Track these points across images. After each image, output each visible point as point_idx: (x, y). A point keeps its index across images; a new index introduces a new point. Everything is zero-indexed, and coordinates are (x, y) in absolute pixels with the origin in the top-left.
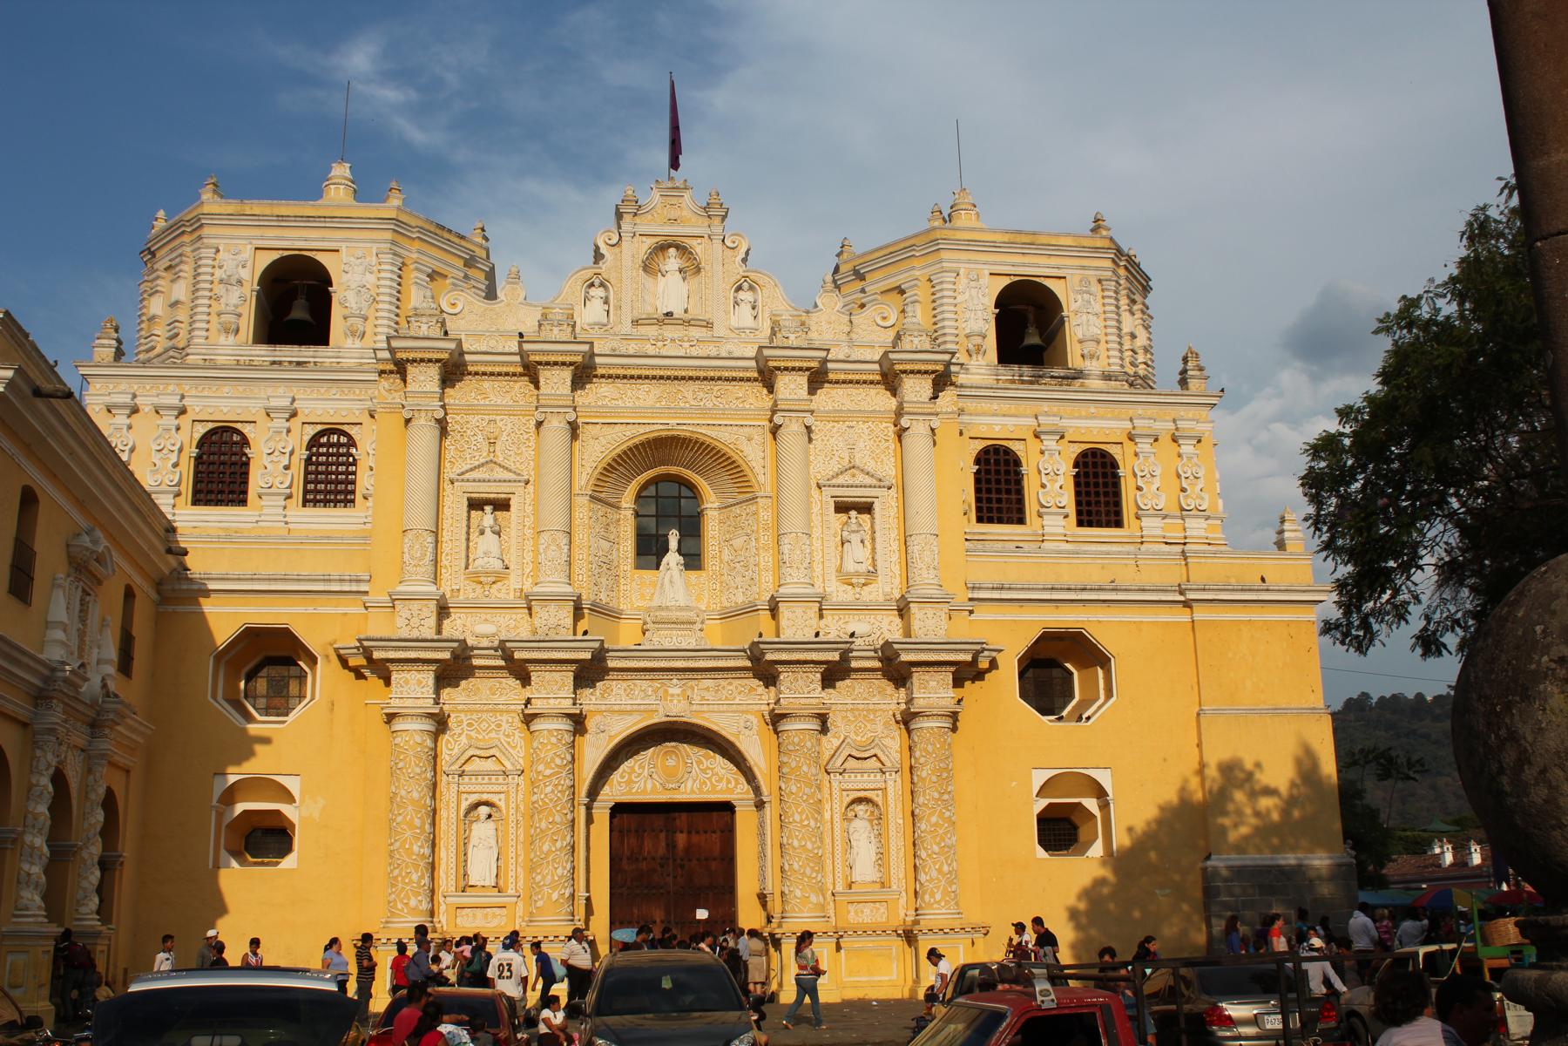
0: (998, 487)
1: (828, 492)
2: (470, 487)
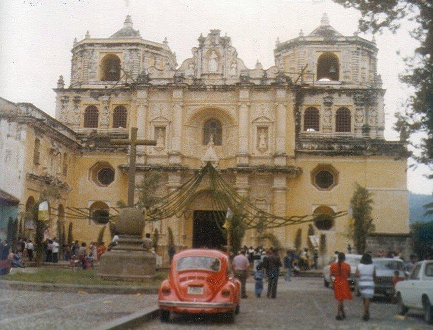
1: (255, 124)
2: (155, 124)
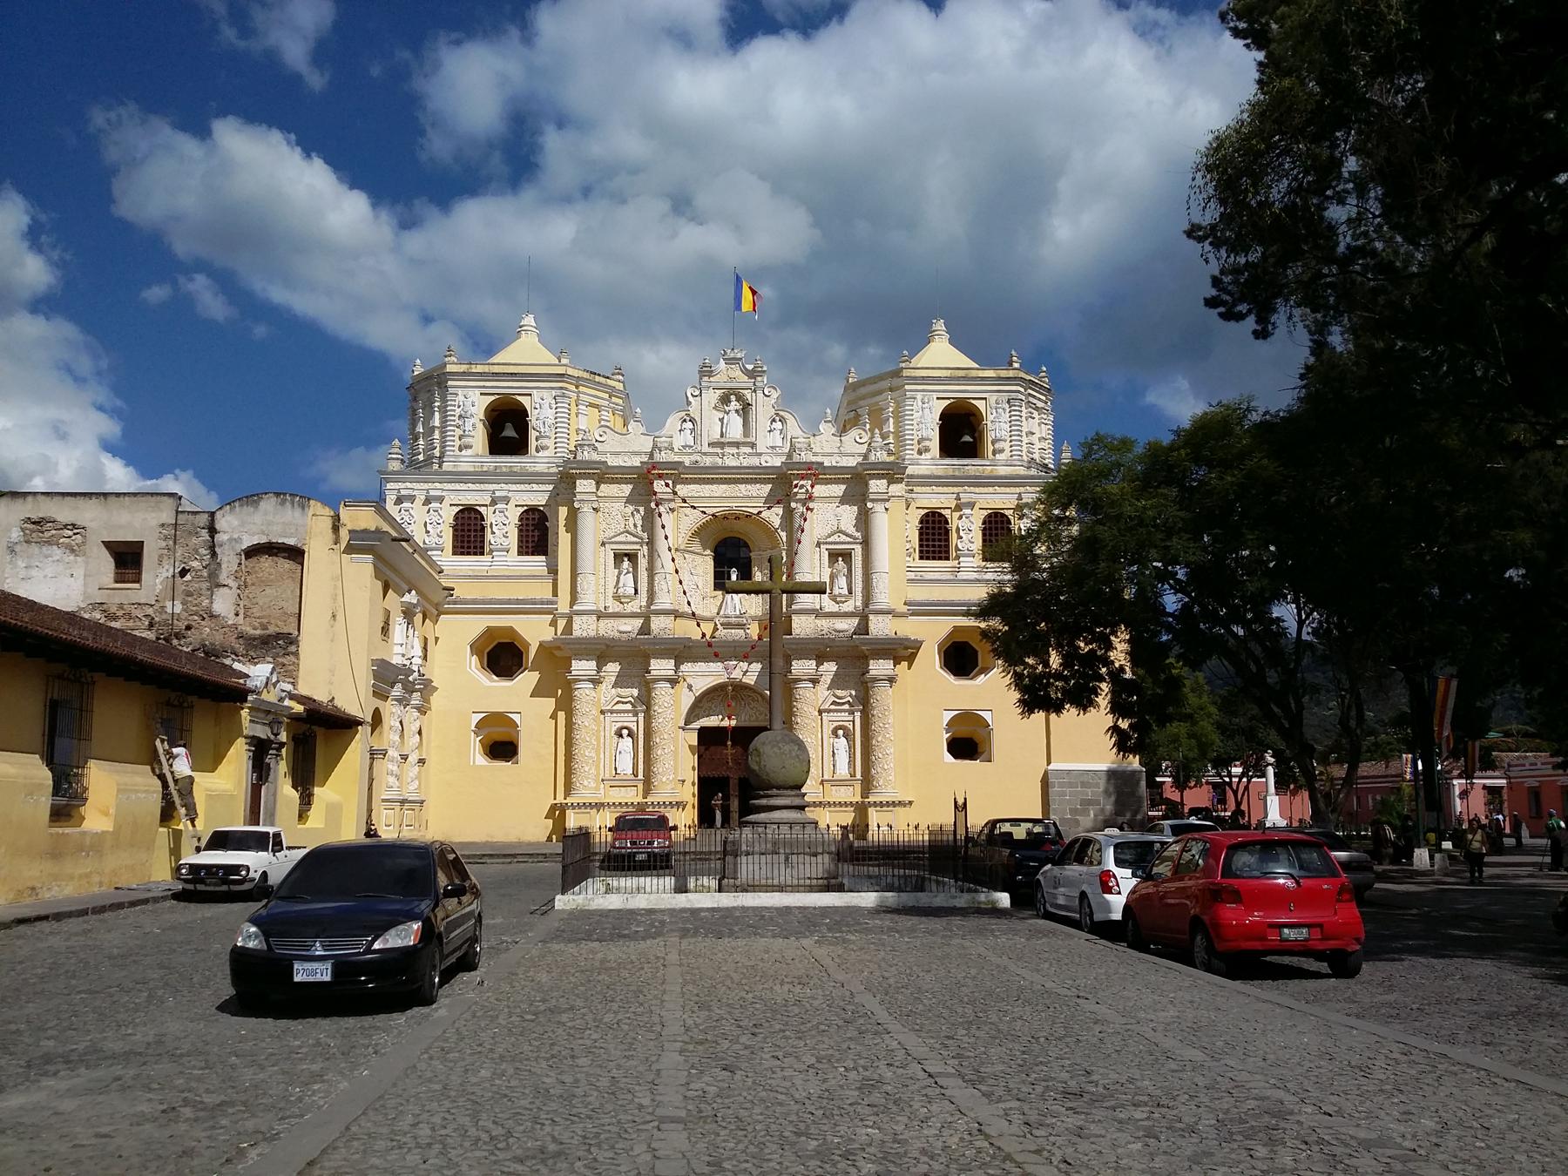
0: (934, 537)
